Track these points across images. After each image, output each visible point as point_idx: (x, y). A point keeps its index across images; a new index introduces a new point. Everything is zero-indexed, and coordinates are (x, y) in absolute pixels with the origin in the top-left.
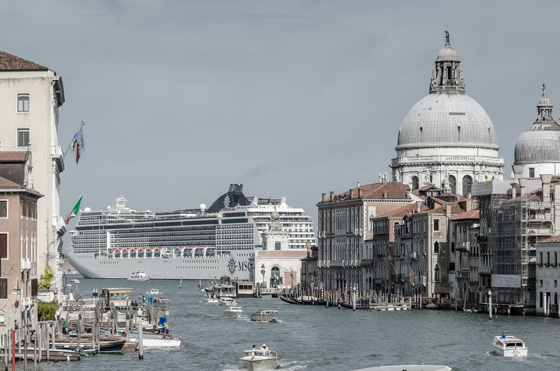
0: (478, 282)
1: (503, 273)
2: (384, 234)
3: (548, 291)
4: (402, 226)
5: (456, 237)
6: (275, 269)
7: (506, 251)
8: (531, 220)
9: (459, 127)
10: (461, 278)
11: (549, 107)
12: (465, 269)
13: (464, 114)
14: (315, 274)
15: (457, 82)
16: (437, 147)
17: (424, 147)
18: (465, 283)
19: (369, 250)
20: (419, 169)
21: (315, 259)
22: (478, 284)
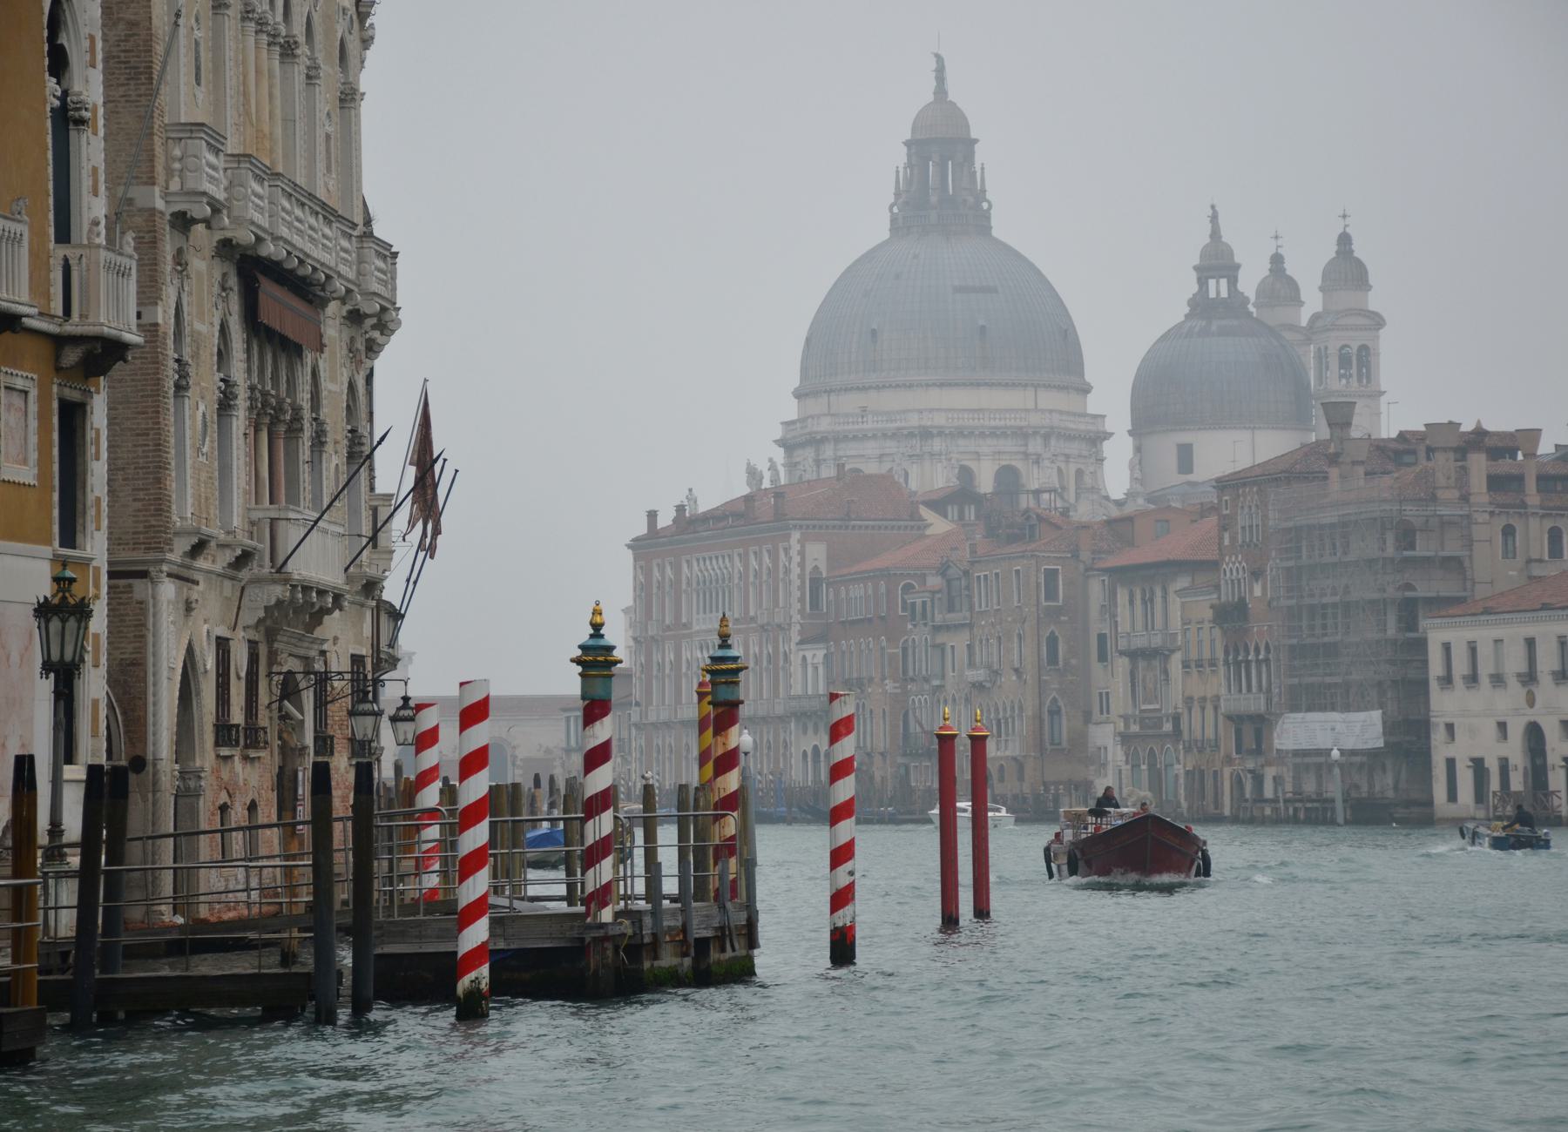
1: (1309, 709)
2: (870, 620)
3: (1477, 754)
4: (933, 593)
5: (1113, 616)
7: (1324, 645)
8: (1407, 553)
9: (983, 327)
10: (1136, 736)
15: (971, 200)
16: (922, 386)
17: (884, 387)
18: (1151, 749)
19: (810, 670)
20: (871, 448)
22: (1217, 746)
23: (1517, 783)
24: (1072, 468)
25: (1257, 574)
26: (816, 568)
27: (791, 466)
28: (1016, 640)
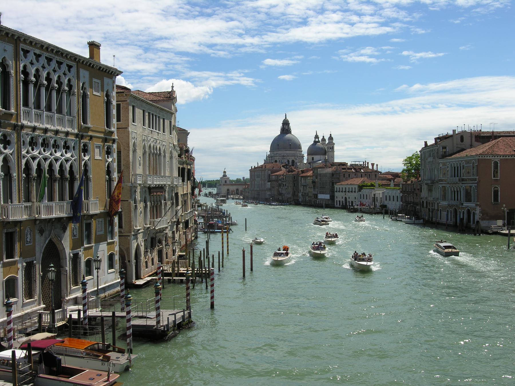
1: (322, 194)
6: (228, 190)
14: (249, 192)
23: (344, 203)
25: (317, 178)
26: (269, 174)
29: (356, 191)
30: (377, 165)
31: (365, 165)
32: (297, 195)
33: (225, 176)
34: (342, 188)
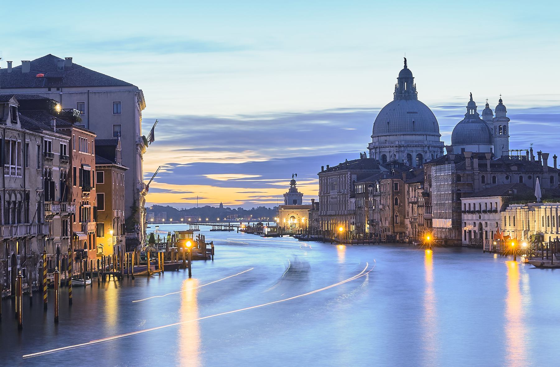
0: (424, 224)
11: (474, 107)
12: (415, 215)
13: (417, 113)
20: (387, 149)
21: (318, 209)
24: (436, 154)
25: (430, 186)
27: (370, 153)
28: (388, 199)
29: (499, 209)
30: (555, 157)
31: (533, 157)
32: (402, 223)
33: (293, 190)
34: (474, 204)
